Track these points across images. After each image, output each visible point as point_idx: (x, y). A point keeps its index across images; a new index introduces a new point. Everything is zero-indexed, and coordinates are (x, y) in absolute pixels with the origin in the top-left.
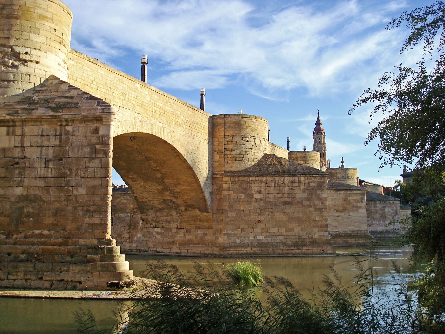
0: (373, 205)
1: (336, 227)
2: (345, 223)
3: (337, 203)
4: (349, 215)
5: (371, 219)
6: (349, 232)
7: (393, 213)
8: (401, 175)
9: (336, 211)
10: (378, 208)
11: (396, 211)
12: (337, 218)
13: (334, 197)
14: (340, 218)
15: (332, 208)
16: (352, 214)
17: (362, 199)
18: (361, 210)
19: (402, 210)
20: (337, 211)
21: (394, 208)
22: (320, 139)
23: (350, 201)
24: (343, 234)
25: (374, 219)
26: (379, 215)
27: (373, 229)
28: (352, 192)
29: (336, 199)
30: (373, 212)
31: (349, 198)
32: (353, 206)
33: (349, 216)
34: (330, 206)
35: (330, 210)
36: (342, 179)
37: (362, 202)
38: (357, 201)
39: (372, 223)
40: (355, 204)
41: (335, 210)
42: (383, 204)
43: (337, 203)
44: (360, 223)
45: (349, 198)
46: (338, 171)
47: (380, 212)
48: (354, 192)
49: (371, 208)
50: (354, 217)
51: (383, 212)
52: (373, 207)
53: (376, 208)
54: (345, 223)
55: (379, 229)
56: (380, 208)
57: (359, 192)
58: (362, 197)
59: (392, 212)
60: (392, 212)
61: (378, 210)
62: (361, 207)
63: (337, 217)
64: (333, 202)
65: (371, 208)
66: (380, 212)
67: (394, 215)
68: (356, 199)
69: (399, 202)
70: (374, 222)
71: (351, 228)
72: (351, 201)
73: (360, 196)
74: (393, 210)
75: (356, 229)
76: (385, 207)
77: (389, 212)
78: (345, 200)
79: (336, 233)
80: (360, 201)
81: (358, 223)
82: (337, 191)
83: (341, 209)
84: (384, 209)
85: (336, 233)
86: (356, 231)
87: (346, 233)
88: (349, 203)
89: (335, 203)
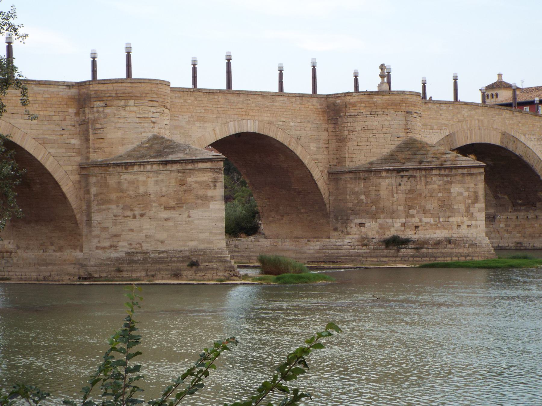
0: (422, 178)
1: (162, 242)
2: (180, 234)
3: (164, 189)
6: (188, 253)
7: (469, 197)
9: (163, 207)
10: (435, 186)
11: (476, 193)
12: (166, 224)
14: (171, 223)
15: (154, 202)
16: (194, 213)
17: (215, 180)
20: (166, 208)
21: (472, 185)
23: (191, 185)
25: (425, 211)
26: (436, 201)
27: (422, 236)
28: (196, 165)
29: (162, 181)
30: (423, 195)
31: (189, 180)
32: (198, 197)
33: (190, 219)
34: (152, 196)
35: (151, 206)
37: (215, 186)
38: (205, 186)
39: (421, 221)
40: (201, 192)
41: (161, 205)
42: (447, 175)
43: (164, 189)
44: (211, 233)
45: (189, 180)
46: (348, 99)
47: (440, 195)
48: (201, 165)
50: (198, 219)
51: (446, 194)
52: (423, 183)
53: (430, 187)
54: (180, 234)
55: (435, 236)
56: (440, 186)
57: (208, 165)
58: (216, 175)
59: (466, 194)
61: (434, 190)
62: (213, 198)
63: (166, 220)
64: (158, 188)
65: (418, 187)
66: (440, 195)
67: (470, 201)
68: (204, 182)
69: (482, 170)
70: (425, 220)
71: (192, 244)
72: (194, 185)
73: (210, 174)
74: (467, 189)
75: (202, 247)
76: (451, 183)
77: (461, 194)
78: (182, 183)
79: (161, 255)
80: (212, 185)
81: (207, 234)
83: (172, 203)
84: (447, 187)
85: (161, 255)
86: (202, 250)
87: (181, 255)
88: (190, 191)
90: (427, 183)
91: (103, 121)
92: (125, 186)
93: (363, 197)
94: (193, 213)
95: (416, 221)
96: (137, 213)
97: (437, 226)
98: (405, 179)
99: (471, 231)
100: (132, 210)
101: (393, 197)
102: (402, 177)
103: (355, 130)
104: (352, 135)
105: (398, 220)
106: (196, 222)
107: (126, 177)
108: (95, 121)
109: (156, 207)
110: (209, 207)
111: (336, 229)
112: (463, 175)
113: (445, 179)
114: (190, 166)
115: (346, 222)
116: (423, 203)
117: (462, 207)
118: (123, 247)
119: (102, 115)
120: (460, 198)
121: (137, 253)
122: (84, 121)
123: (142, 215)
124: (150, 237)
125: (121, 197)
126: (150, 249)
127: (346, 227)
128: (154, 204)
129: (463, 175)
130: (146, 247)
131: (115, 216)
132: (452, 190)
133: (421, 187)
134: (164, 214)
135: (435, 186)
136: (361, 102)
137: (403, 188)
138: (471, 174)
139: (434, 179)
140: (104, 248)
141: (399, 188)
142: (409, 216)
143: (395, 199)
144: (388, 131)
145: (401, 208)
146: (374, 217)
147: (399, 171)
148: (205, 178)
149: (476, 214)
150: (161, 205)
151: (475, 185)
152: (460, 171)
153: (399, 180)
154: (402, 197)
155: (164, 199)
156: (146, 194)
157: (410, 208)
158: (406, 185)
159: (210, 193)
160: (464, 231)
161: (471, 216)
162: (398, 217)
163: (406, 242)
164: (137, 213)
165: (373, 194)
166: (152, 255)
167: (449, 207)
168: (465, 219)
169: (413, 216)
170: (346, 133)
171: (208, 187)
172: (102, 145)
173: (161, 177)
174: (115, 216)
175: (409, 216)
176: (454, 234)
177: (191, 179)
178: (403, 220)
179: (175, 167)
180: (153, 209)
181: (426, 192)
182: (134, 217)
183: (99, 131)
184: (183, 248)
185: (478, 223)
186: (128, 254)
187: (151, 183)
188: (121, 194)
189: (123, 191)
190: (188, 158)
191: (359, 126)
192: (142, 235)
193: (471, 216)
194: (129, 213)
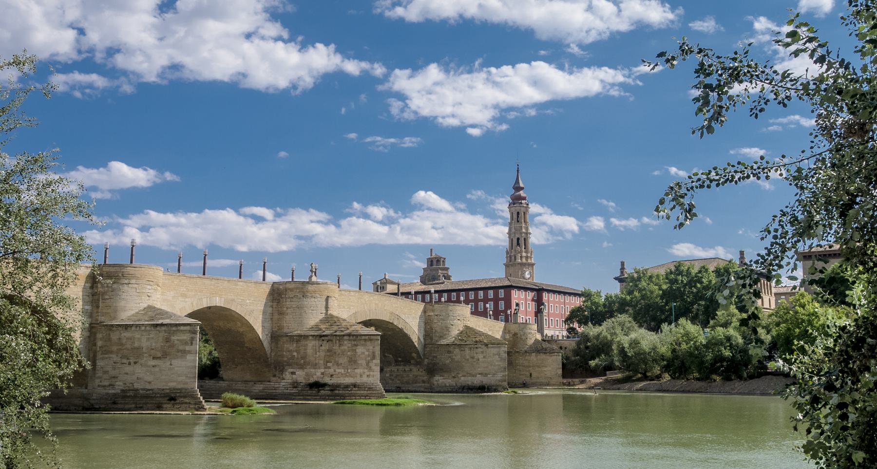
0: (337, 342)
1: (150, 383)
3: (154, 344)
4: (171, 365)
5: (333, 365)
6: (168, 391)
7: (369, 356)
8: (616, 279)
10: (346, 348)
11: (374, 353)
12: (153, 369)
13: (151, 336)
14: (157, 369)
15: (146, 353)
17: (192, 339)
18: (189, 357)
19: (492, 346)
20: (154, 358)
21: (371, 348)
22: (518, 213)
24: (158, 394)
25: (338, 365)
26: (346, 358)
27: (335, 382)
28: (179, 328)
29: (153, 338)
30: (337, 353)
31: (173, 338)
32: (178, 351)
35: (143, 356)
36: (293, 300)
37: (192, 343)
39: (335, 371)
40: (181, 348)
42: (354, 340)
43: (154, 344)
44: (187, 377)
45: (173, 338)
46: (288, 286)
48: (182, 328)
49: (334, 348)
50: (177, 367)
52: (338, 345)
55: (344, 382)
57: (188, 328)
58: (193, 335)
59: (367, 353)
60: (367, 353)
62: (190, 352)
64: (148, 343)
65: (334, 348)
66: (349, 353)
67: (369, 358)
68: (183, 340)
69: (379, 338)
71: (172, 385)
72: (176, 342)
73: (189, 334)
74: (368, 350)
75: (179, 387)
76: (357, 345)
77: (363, 353)
78: (168, 340)
80: (189, 342)
81: (184, 378)
82: (156, 327)
83: (159, 355)
84: (354, 348)
86: (179, 389)
88: (172, 346)
89: (151, 346)
90: (340, 345)
91: (111, 294)
92: (124, 341)
93: (295, 354)
94: (174, 362)
95: (331, 371)
96: (132, 361)
97: (346, 375)
98: (325, 342)
99: (370, 379)
100: (128, 359)
101: (316, 354)
102: (323, 340)
103: (291, 307)
104: (289, 311)
105: (319, 370)
106: (176, 368)
107: (125, 334)
108: (104, 293)
109: (146, 357)
110: (186, 358)
111: (275, 376)
112: (365, 340)
113: (353, 343)
114: (174, 329)
115: (282, 371)
116: (337, 359)
117: (364, 362)
118: (119, 386)
119: (110, 289)
120: (363, 356)
121: (129, 390)
122: (96, 293)
123: (135, 363)
124: (140, 379)
125: (120, 349)
126: (140, 387)
127: (282, 374)
128: (145, 355)
129: (365, 340)
130: (136, 386)
131: (115, 363)
132: (357, 350)
133: (336, 347)
134: (152, 362)
135: (346, 348)
136: (297, 288)
137: (323, 348)
138: (371, 340)
139: (345, 342)
140: (104, 386)
141: (321, 348)
142: (326, 367)
143: (317, 356)
144: (315, 309)
145: (321, 362)
146: (302, 367)
147: (321, 336)
148: (185, 338)
149: (374, 367)
150: (151, 355)
151: (374, 347)
152: (363, 337)
153: (321, 343)
154: (322, 354)
155: (152, 351)
156: (139, 348)
157: (328, 362)
158: (326, 346)
159: (188, 348)
160: (365, 379)
161: (370, 369)
162: (319, 368)
163: (324, 385)
164: (132, 361)
165: (302, 352)
166: (141, 392)
167: (355, 362)
168: (366, 370)
169: (329, 368)
170: (285, 309)
171: (186, 343)
172: (109, 311)
173: (151, 336)
174: (115, 363)
175: (326, 367)
176: (358, 380)
177: (174, 338)
178: (323, 370)
179: (163, 328)
180: (145, 359)
181: (339, 351)
182: (130, 364)
183: (107, 301)
184: (165, 387)
185: (375, 373)
186: (123, 391)
187: (144, 339)
188: (120, 347)
189: (122, 344)
190: (173, 322)
191: (294, 304)
192: (135, 377)
193: (370, 369)
194: (125, 361)
